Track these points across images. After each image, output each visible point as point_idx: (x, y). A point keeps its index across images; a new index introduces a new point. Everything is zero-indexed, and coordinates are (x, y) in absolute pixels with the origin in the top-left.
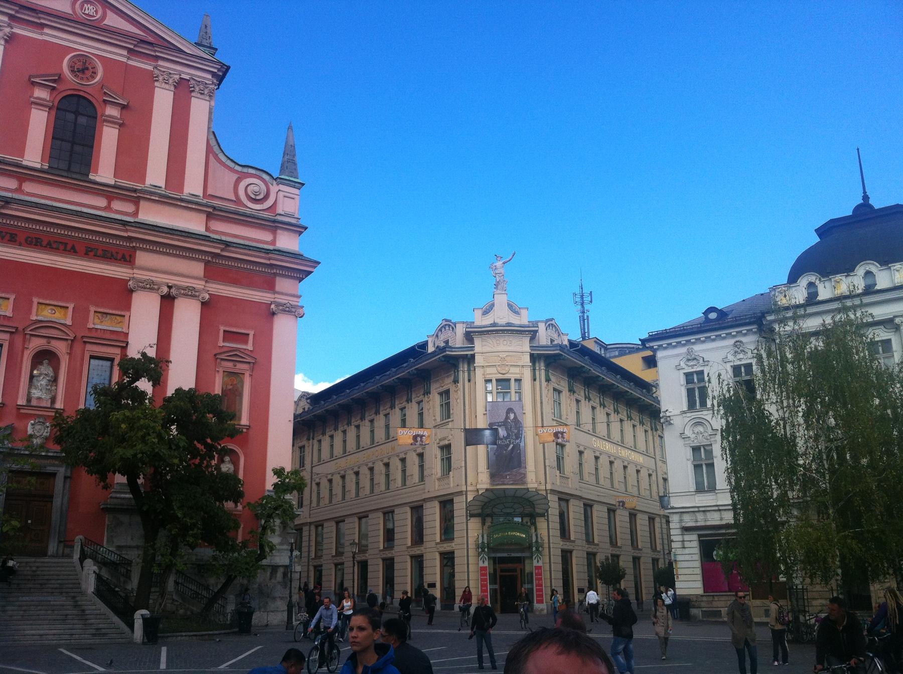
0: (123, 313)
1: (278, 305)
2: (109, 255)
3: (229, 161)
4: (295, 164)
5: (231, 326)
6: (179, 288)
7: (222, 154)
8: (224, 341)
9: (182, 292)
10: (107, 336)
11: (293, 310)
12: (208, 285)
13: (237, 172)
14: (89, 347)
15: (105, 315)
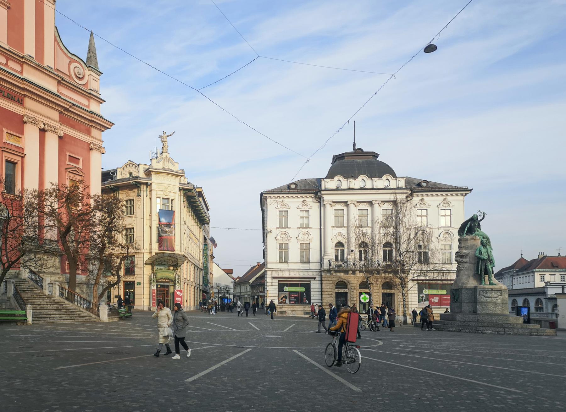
0: (20, 136)
1: (94, 145)
2: (11, 97)
3: (65, 49)
4: (96, 59)
5: (72, 153)
6: (49, 126)
7: (61, 43)
8: (69, 161)
9: (50, 128)
10: (14, 148)
11: (100, 149)
12: (62, 127)
13: (68, 57)
14: (5, 154)
15: (10, 135)
